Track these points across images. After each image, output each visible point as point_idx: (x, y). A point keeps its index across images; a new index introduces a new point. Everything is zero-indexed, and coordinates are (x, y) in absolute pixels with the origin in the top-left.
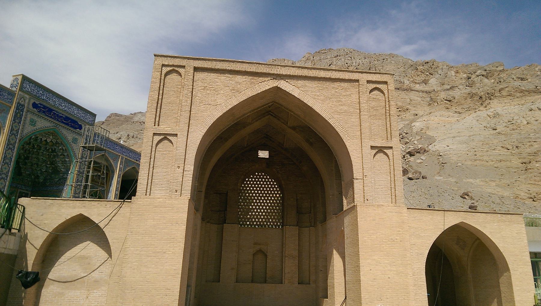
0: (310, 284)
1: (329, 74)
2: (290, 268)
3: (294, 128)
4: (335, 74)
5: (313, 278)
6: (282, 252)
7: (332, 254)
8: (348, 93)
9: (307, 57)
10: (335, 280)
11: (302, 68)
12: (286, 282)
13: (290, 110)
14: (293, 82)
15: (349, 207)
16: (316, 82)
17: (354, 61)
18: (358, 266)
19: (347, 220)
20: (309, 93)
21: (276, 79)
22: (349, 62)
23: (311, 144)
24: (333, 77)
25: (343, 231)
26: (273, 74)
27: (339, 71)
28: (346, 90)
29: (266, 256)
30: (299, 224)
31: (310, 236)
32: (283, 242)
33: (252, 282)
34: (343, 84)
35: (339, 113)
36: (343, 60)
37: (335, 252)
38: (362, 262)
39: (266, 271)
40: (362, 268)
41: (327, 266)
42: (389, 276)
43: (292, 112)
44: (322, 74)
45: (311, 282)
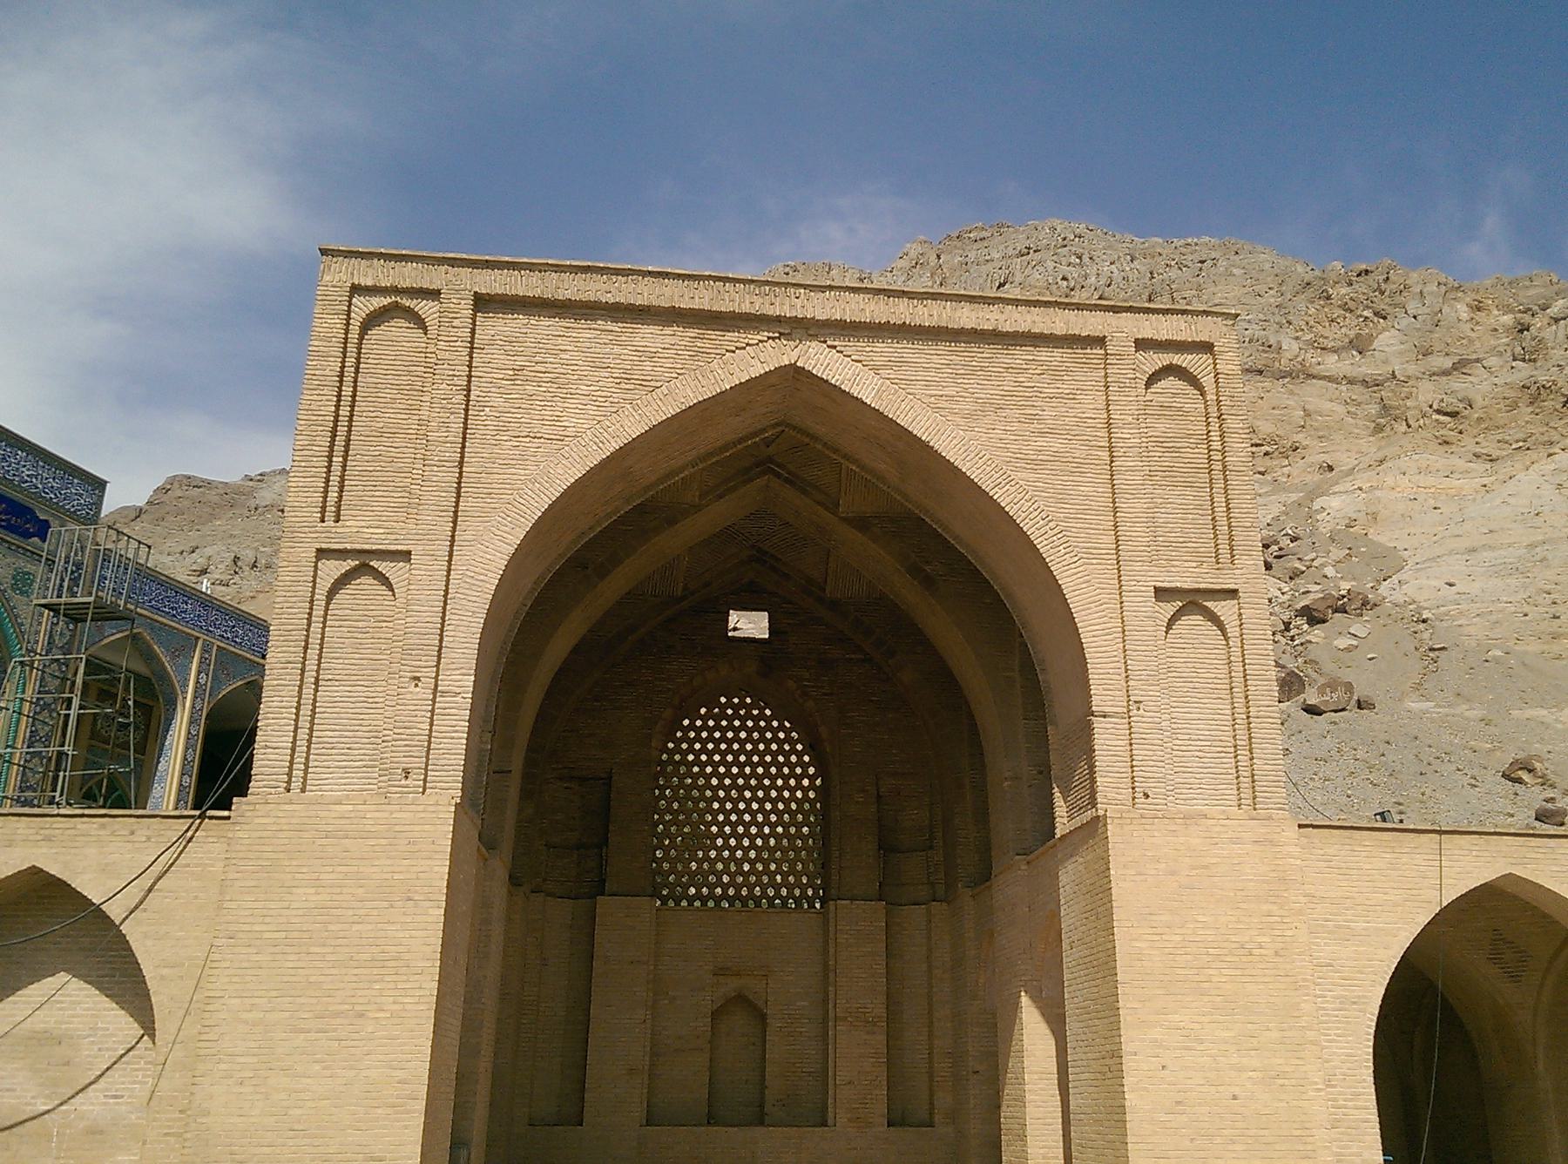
0: (931, 1125)
1: (993, 316)
2: (856, 1063)
3: (861, 523)
4: (1016, 316)
5: (944, 1100)
6: (825, 1001)
7: (1016, 1006)
8: (1065, 388)
9: (913, 254)
10: (1030, 1111)
11: (889, 293)
12: (842, 1118)
13: (845, 456)
14: (855, 347)
15: (1077, 822)
16: (943, 347)
17: (1092, 270)
18: (1116, 1055)
19: (1069, 876)
20: (917, 389)
21: (788, 336)
22: (1074, 273)
23: (928, 582)
24: (1008, 328)
25: (1055, 916)
26: (779, 320)
27: (1028, 303)
28: (1056, 374)
29: (763, 1018)
30: (887, 892)
31: (929, 938)
32: (826, 965)
33: (711, 1119)
34: (1044, 354)
35: (1035, 464)
36: (1050, 265)
37: (1025, 1000)
38: (1131, 1039)
39: (763, 1076)
40: (1128, 1063)
41: (996, 1054)
42: (1237, 1091)
43: (855, 461)
44: (966, 316)
45: (937, 1118)
